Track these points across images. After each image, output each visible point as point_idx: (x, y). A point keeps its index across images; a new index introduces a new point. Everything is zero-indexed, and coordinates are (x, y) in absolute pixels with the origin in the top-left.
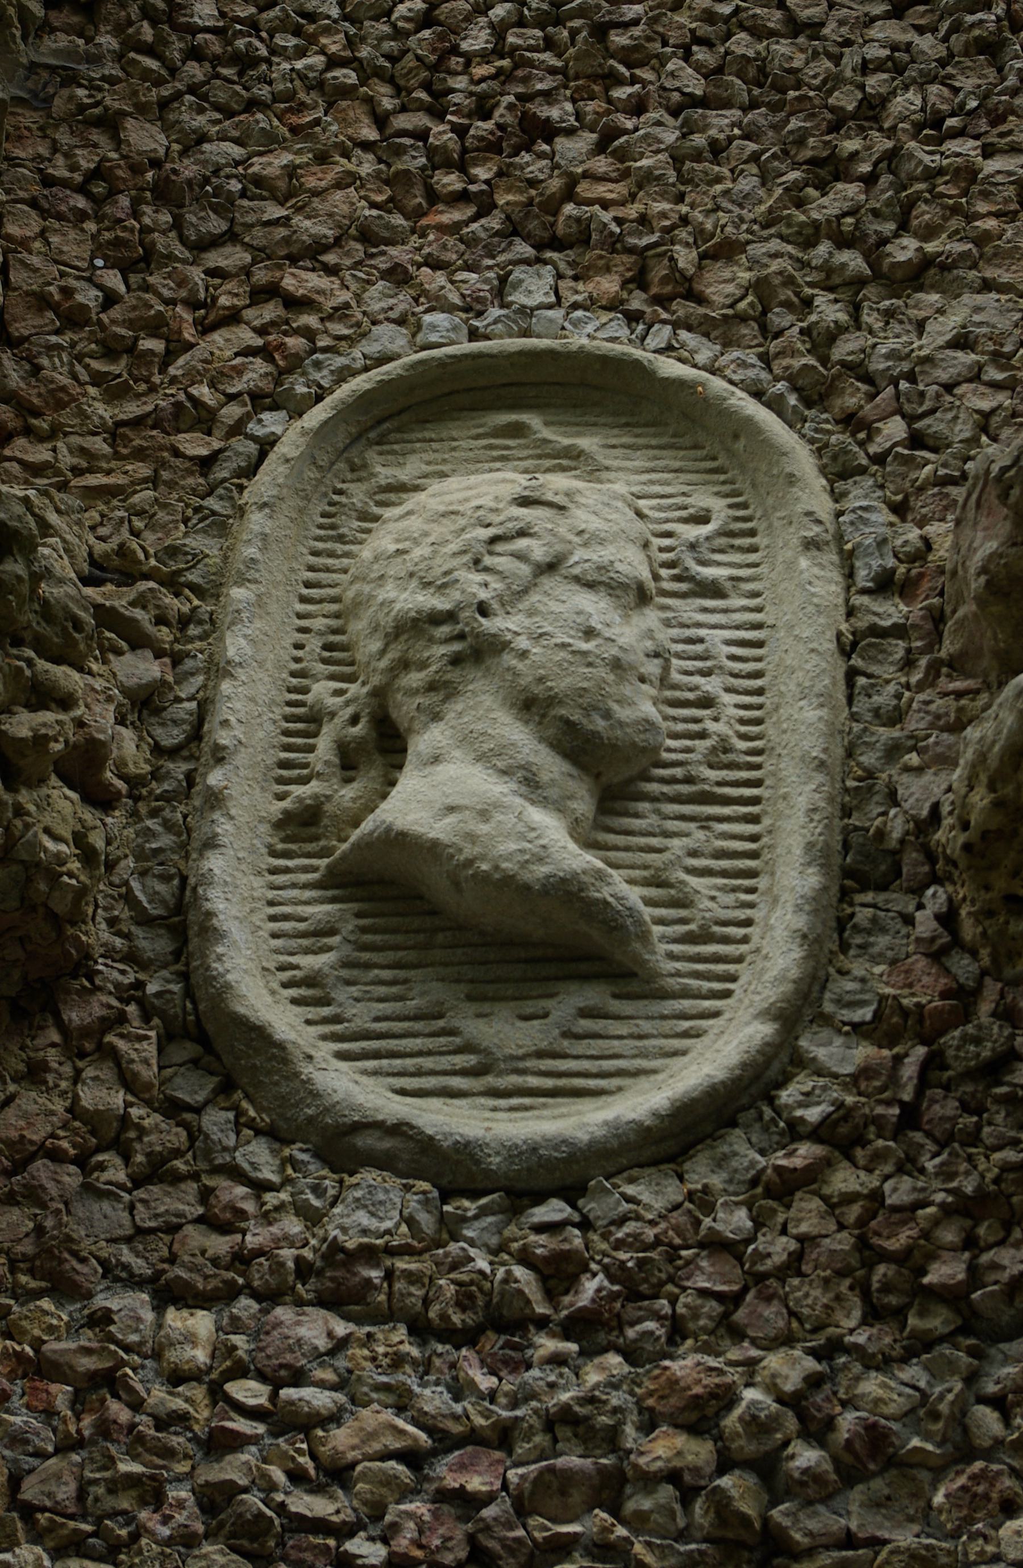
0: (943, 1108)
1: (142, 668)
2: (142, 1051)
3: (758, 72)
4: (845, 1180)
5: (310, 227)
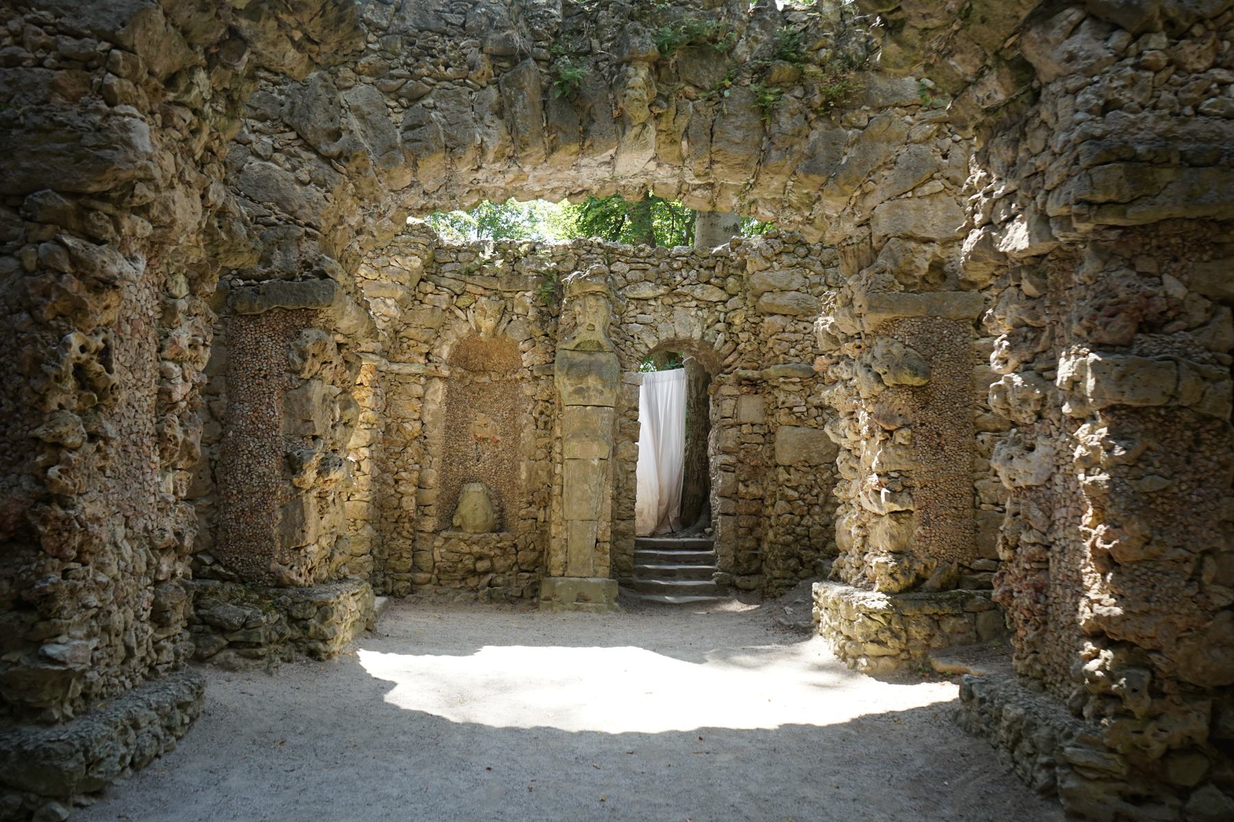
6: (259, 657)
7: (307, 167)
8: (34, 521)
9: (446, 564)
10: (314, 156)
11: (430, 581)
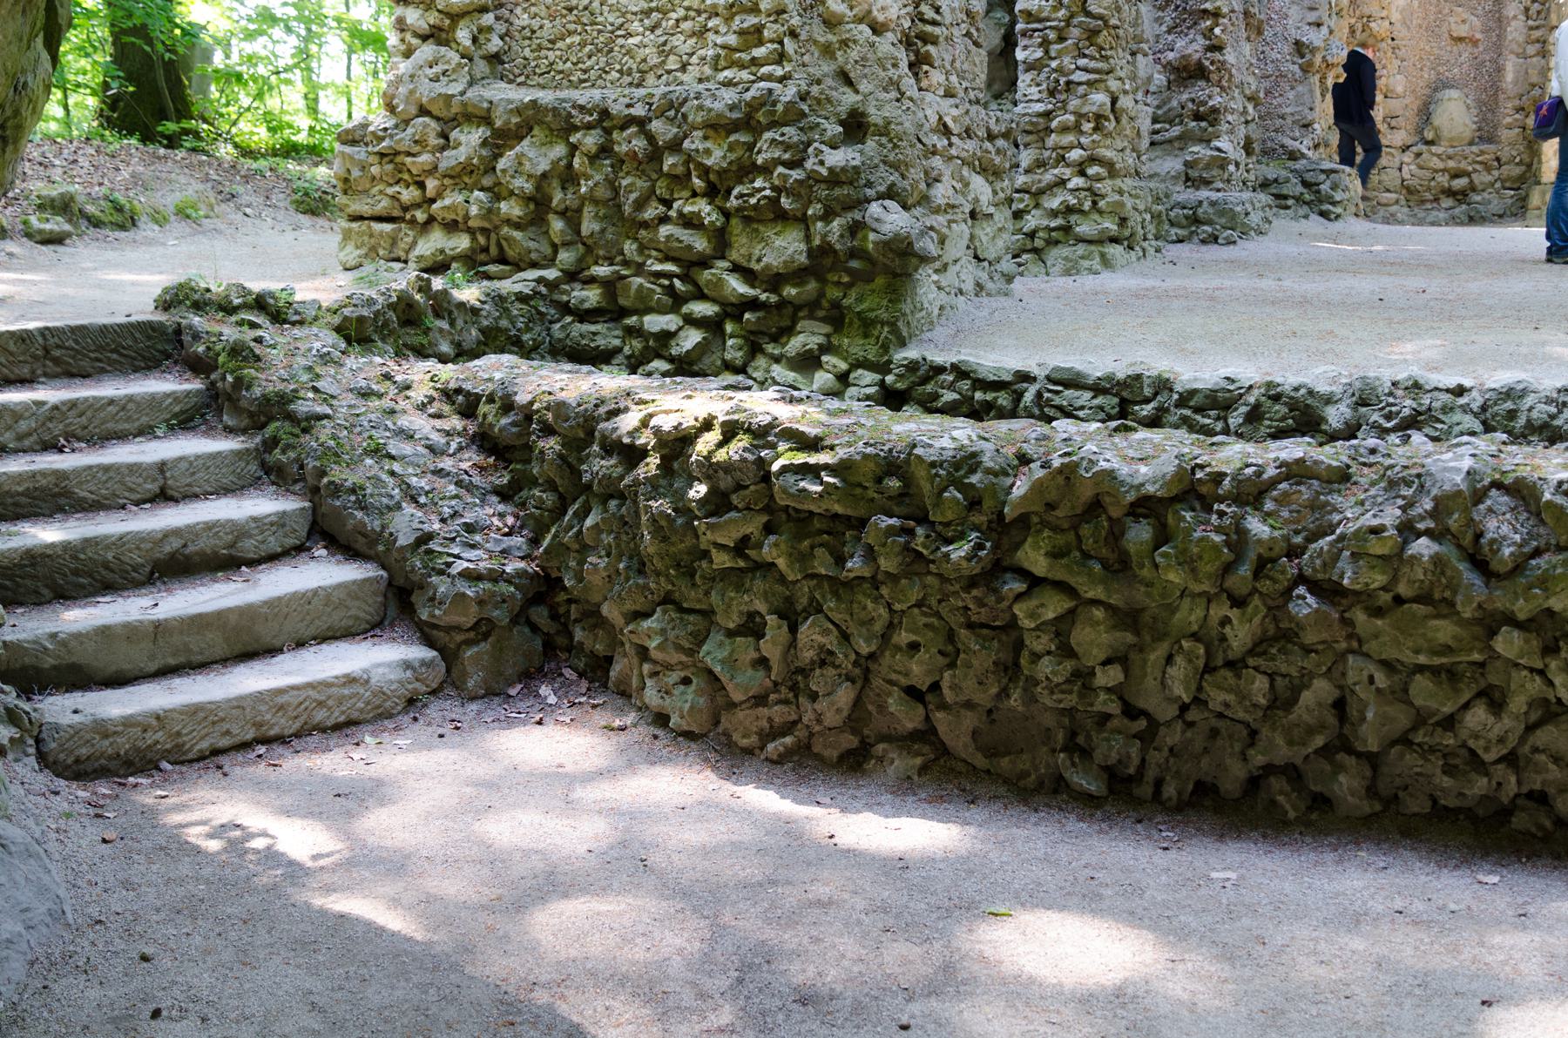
6: (1287, 208)
8: (1207, 63)
9: (1414, 182)
11: (1397, 202)
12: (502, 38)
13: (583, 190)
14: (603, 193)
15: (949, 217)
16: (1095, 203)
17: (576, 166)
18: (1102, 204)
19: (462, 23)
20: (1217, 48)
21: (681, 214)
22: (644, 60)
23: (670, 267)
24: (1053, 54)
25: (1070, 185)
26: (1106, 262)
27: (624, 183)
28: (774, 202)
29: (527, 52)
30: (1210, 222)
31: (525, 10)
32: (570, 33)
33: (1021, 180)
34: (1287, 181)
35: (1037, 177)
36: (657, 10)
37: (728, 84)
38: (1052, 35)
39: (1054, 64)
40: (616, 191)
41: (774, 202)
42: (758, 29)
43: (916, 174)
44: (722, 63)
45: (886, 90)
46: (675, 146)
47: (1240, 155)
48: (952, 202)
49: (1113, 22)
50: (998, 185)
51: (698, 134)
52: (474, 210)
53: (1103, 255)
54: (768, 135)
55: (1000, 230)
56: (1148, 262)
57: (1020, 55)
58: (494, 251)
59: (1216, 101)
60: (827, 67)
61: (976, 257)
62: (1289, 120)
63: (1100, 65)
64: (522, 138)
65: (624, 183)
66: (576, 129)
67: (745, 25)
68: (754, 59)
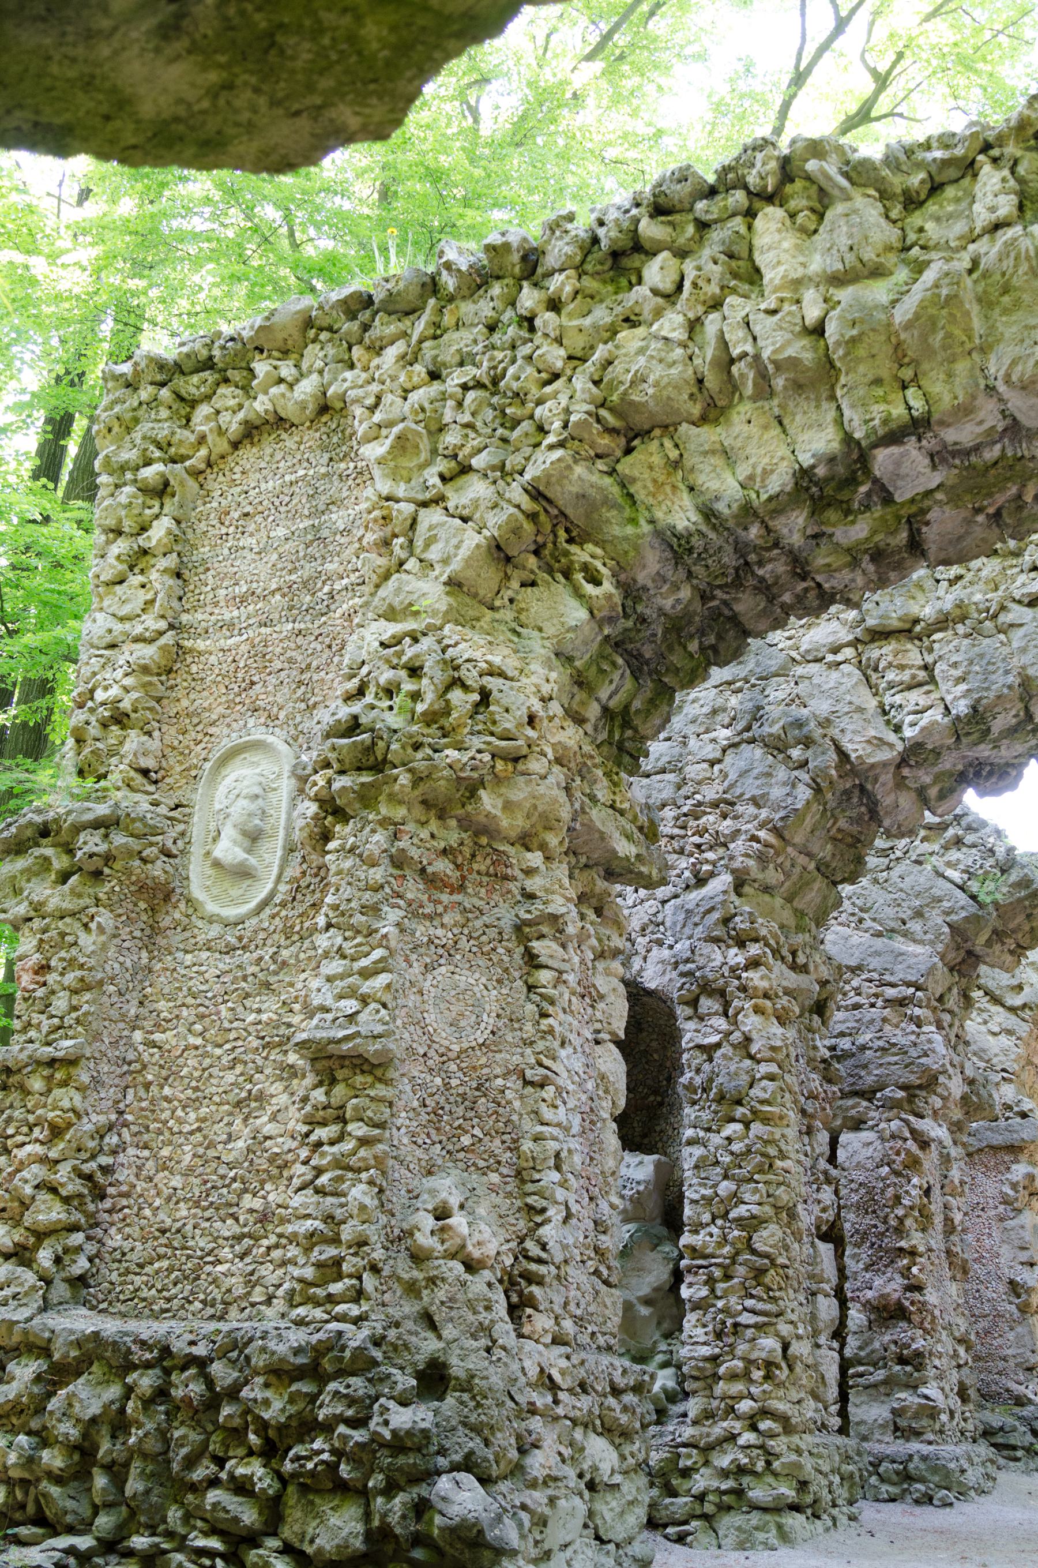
0: (299, 896)
1: (181, 827)
2: (182, 905)
3: (291, 661)
4: (283, 913)
5: (214, 717)
6: (1017, 1459)
7: (998, 1019)
8: (907, 1303)
10: (1001, 1009)
12: (91, 1260)
13: (132, 1440)
14: (153, 1445)
15: (550, 1492)
16: (768, 1463)
17: (129, 1411)
18: (776, 1465)
19: (46, 1243)
20: (918, 1288)
21: (232, 1476)
22: (229, 1291)
23: (214, 1543)
24: (719, 1293)
25: (741, 1441)
26: (784, 1536)
27: (177, 1434)
28: (332, 1468)
29: (114, 1277)
30: (922, 1480)
31: (119, 1230)
32: (160, 1257)
33: (688, 1432)
34: (1014, 1429)
35: (705, 1430)
36: (250, 1236)
37: (300, 1323)
38: (718, 1273)
39: (720, 1304)
40: (166, 1441)
41: (332, 1468)
42: (337, 1262)
43: (505, 1440)
44: (297, 1299)
45: (474, 1337)
46: (233, 1393)
47: (955, 1402)
48: (554, 1473)
49: (780, 1260)
50: (627, 1449)
51: (260, 1380)
52: (12, 1458)
53: (780, 1527)
54: (332, 1386)
55: (631, 1503)
56: (838, 1535)
57: (685, 1292)
58: (31, 1509)
59: (919, 1344)
60: (410, 1307)
61: (598, 1538)
62: (1012, 1363)
63: (768, 1307)
64: (79, 1374)
65: (177, 1434)
66: (135, 1367)
67: (323, 1257)
68: (329, 1295)
